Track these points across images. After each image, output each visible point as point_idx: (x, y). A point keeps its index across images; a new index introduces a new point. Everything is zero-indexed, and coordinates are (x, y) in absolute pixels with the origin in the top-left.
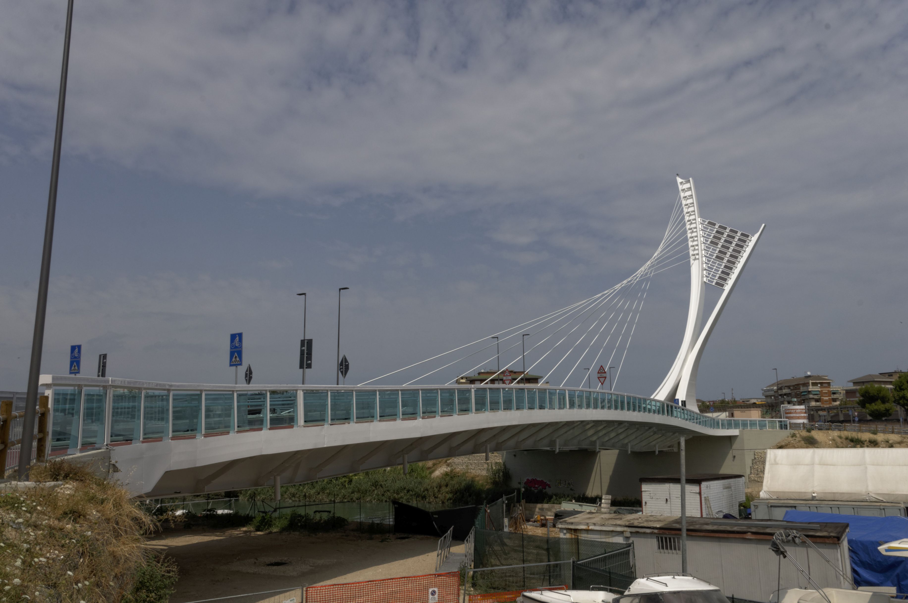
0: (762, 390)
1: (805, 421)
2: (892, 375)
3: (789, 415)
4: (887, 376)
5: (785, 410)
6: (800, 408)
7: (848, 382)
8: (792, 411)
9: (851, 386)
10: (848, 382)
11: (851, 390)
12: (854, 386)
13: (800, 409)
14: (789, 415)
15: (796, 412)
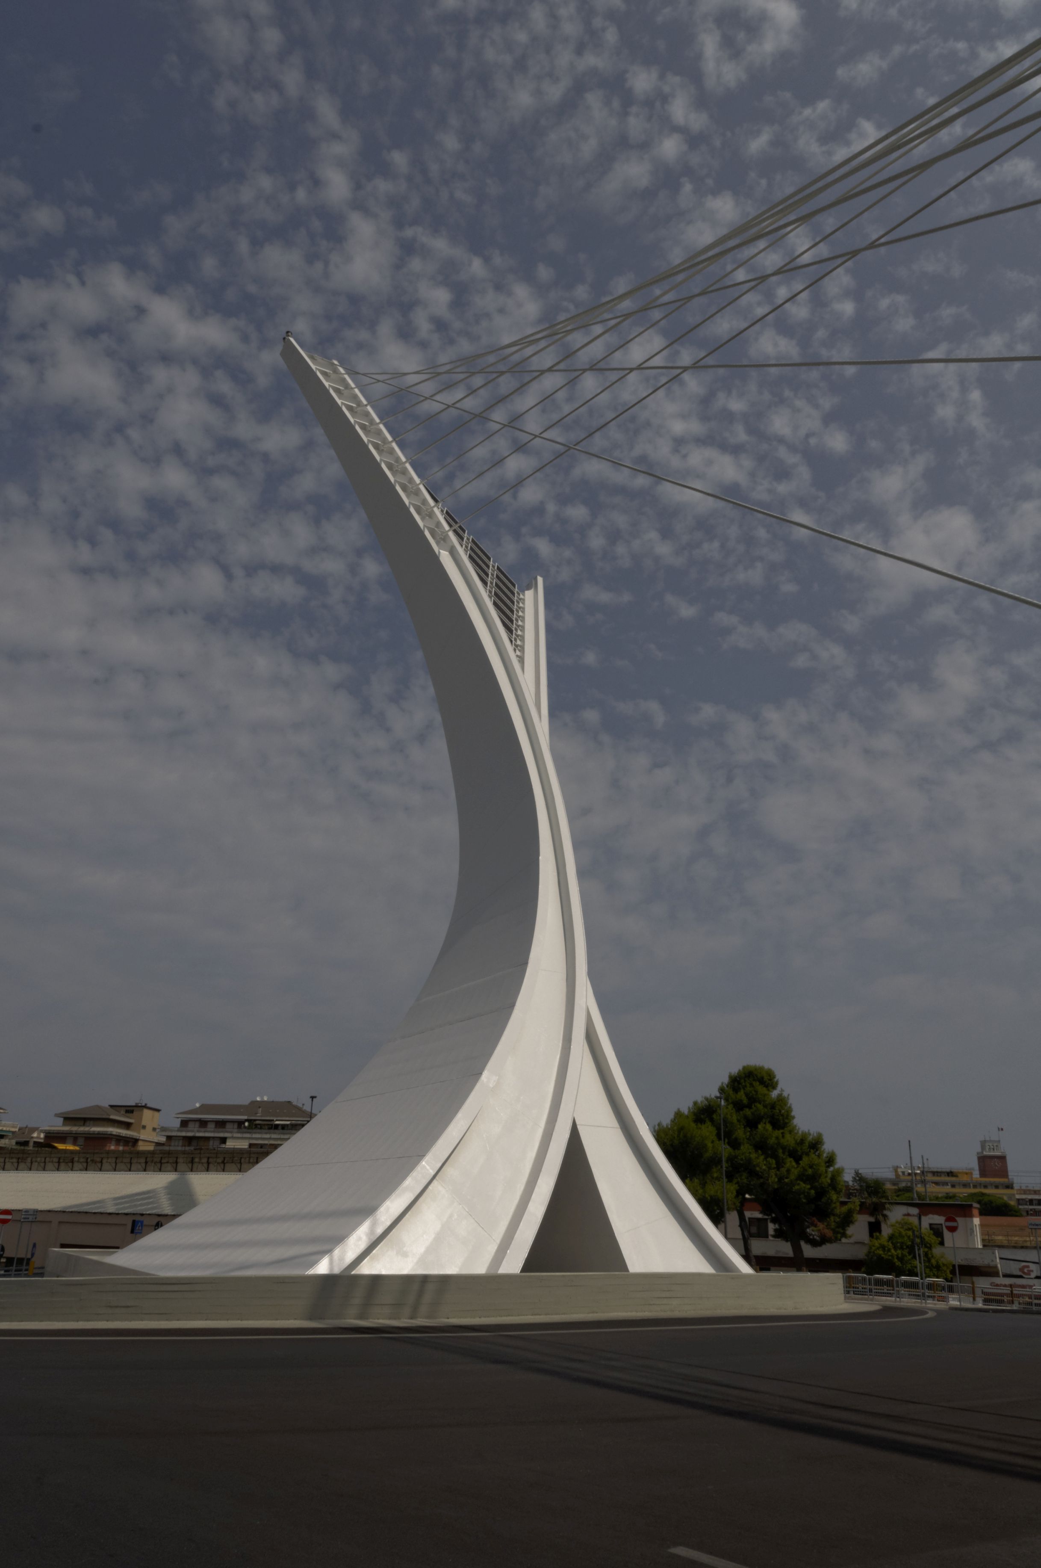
2: (132, 1112)
4: (123, 1112)
7: (57, 1115)
9: (58, 1126)
10: (57, 1115)
11: (58, 1133)
12: (64, 1125)
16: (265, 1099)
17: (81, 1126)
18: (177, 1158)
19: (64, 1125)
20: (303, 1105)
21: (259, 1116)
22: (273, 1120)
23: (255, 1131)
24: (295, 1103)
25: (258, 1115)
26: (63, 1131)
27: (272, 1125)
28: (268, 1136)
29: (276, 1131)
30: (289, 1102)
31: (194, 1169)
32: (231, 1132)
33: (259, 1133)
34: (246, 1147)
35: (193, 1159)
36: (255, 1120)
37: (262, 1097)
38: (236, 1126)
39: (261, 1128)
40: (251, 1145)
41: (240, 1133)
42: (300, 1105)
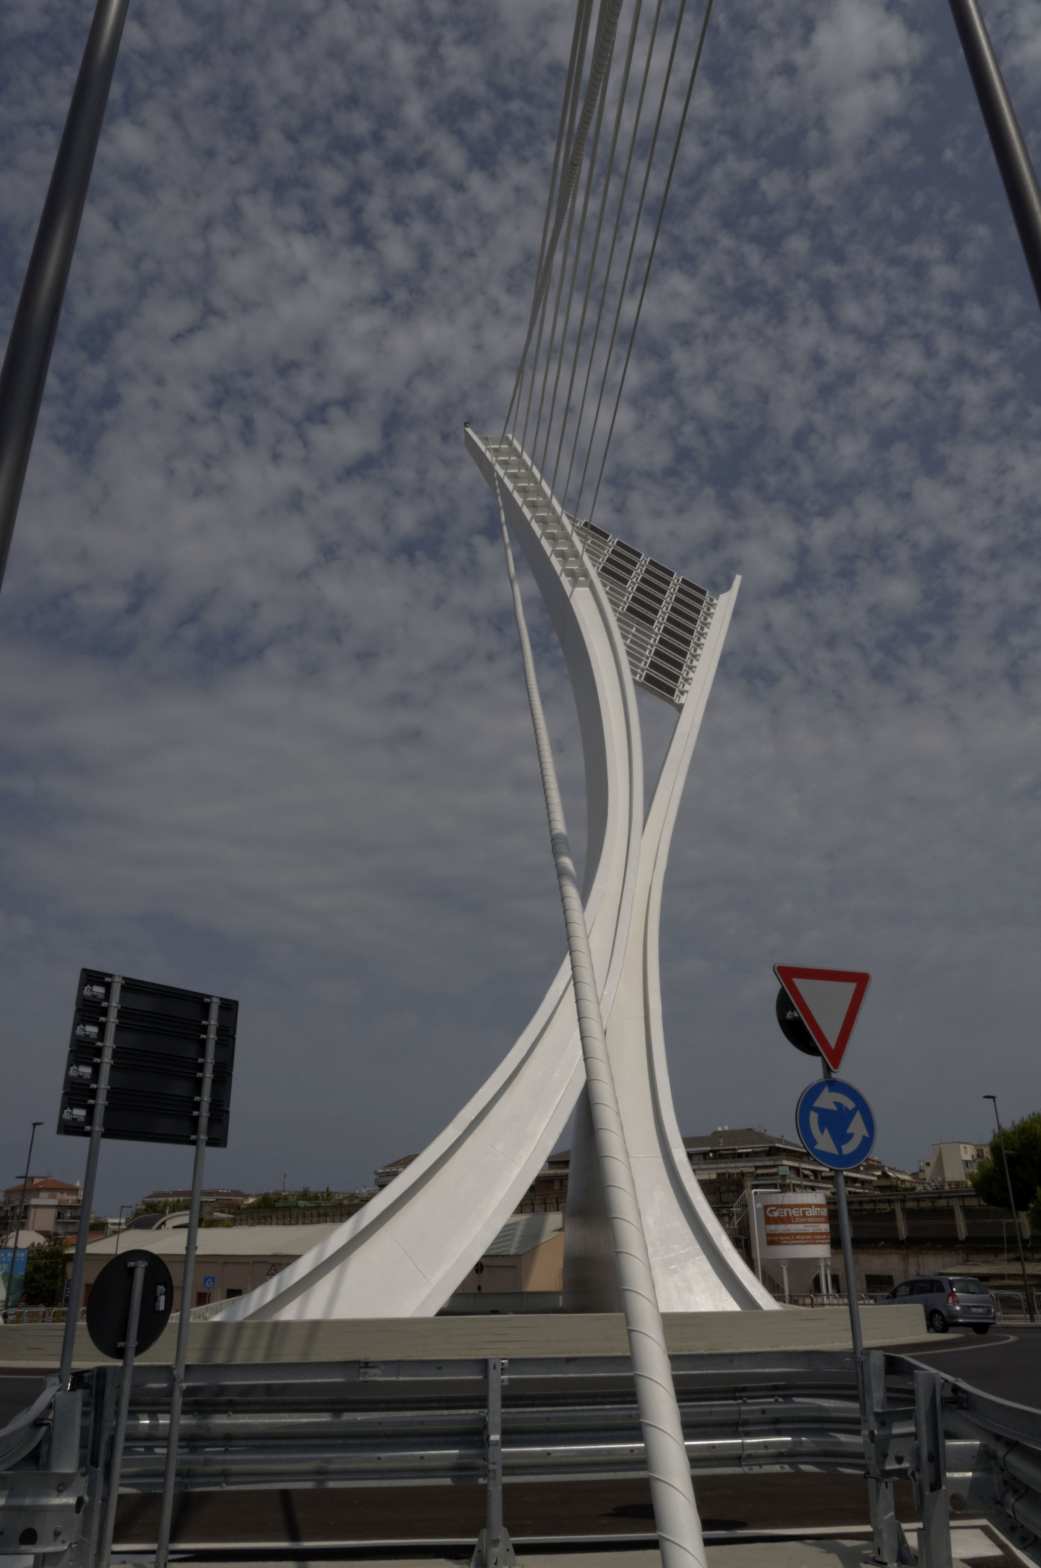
0: (376, 1173)
1: (821, 1251)
3: (781, 1228)
5: (766, 1207)
6: (815, 1202)
8: (794, 1212)
12: (550, 1168)
13: (817, 1206)
14: (781, 1228)
15: (804, 1216)
16: (726, 1128)
17: (564, 1168)
18: (533, 1200)
19: (550, 1168)
20: (765, 1131)
21: (721, 1146)
22: (735, 1149)
23: (719, 1161)
24: (757, 1130)
25: (721, 1145)
26: (550, 1174)
27: (735, 1154)
28: (733, 1165)
29: (740, 1159)
30: (751, 1129)
31: (548, 1210)
32: (698, 1164)
33: (724, 1163)
34: (714, 1176)
35: (545, 1200)
36: (719, 1150)
37: (723, 1128)
38: (702, 1157)
39: (725, 1158)
40: (718, 1175)
41: (707, 1164)
42: (763, 1131)
